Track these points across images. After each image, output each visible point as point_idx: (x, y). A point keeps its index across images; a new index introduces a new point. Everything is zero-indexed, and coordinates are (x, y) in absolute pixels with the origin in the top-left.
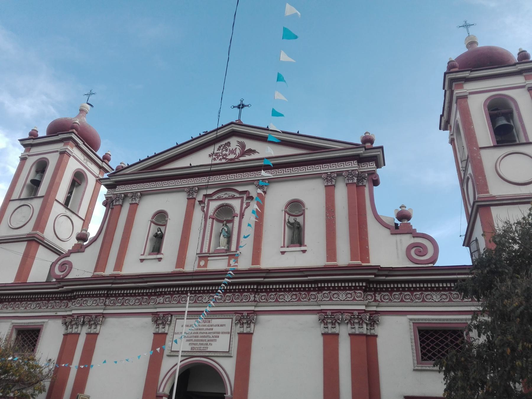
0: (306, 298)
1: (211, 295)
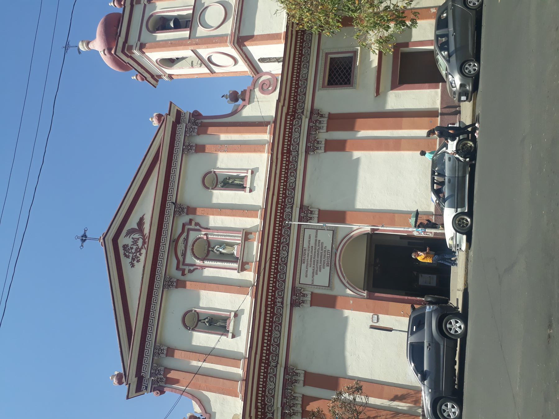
0: (294, 165)
1: (281, 249)
